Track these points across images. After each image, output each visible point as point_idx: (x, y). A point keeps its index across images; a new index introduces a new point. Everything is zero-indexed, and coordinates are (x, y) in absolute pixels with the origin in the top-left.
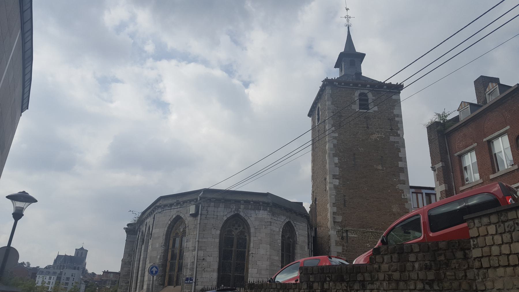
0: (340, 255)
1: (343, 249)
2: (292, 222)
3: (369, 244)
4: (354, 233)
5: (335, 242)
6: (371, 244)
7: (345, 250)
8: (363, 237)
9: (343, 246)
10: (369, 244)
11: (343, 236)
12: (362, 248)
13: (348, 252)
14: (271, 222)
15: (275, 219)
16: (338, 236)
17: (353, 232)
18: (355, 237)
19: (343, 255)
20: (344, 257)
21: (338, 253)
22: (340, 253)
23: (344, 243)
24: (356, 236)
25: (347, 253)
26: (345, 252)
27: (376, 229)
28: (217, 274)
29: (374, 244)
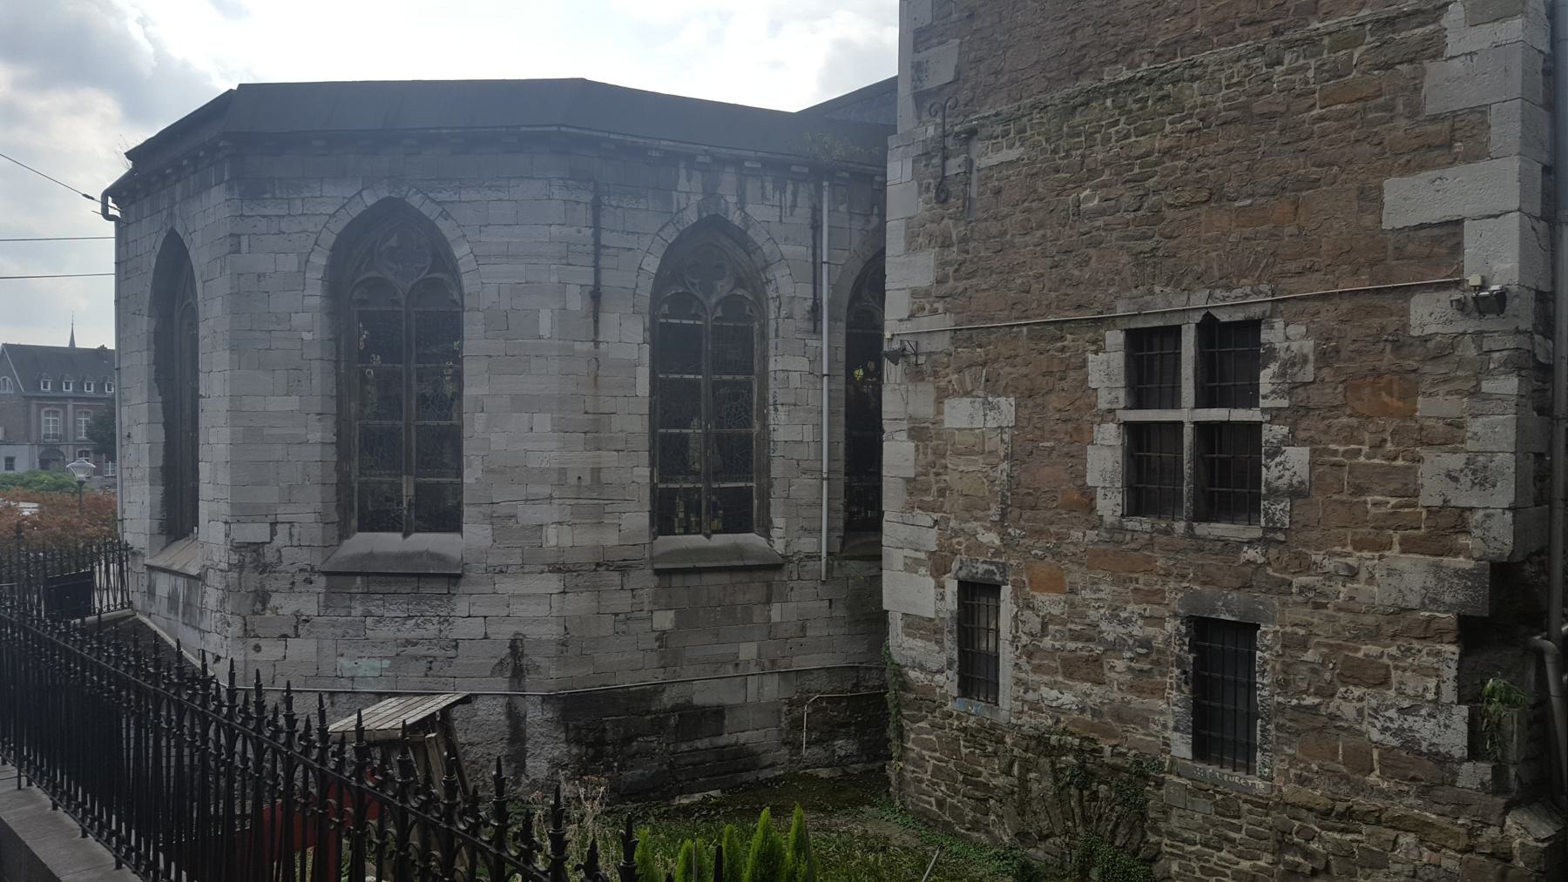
0: (928, 307)
1: (943, 264)
2: (415, 200)
3: (1095, 188)
4: (1006, 134)
5: (903, 233)
6: (1104, 185)
7: (950, 270)
8: (1055, 152)
9: (946, 244)
10: (1095, 188)
11: (944, 177)
12: (1049, 233)
13: (970, 275)
14: (238, 236)
15: (267, 212)
16: (920, 185)
17: (999, 129)
18: (1011, 163)
19: (940, 306)
20: (946, 311)
21: (915, 293)
22: (927, 293)
23: (951, 222)
24: (1012, 154)
25: (961, 285)
26: (951, 282)
27: (1171, 48)
28: (160, 489)
29: (1128, 176)
